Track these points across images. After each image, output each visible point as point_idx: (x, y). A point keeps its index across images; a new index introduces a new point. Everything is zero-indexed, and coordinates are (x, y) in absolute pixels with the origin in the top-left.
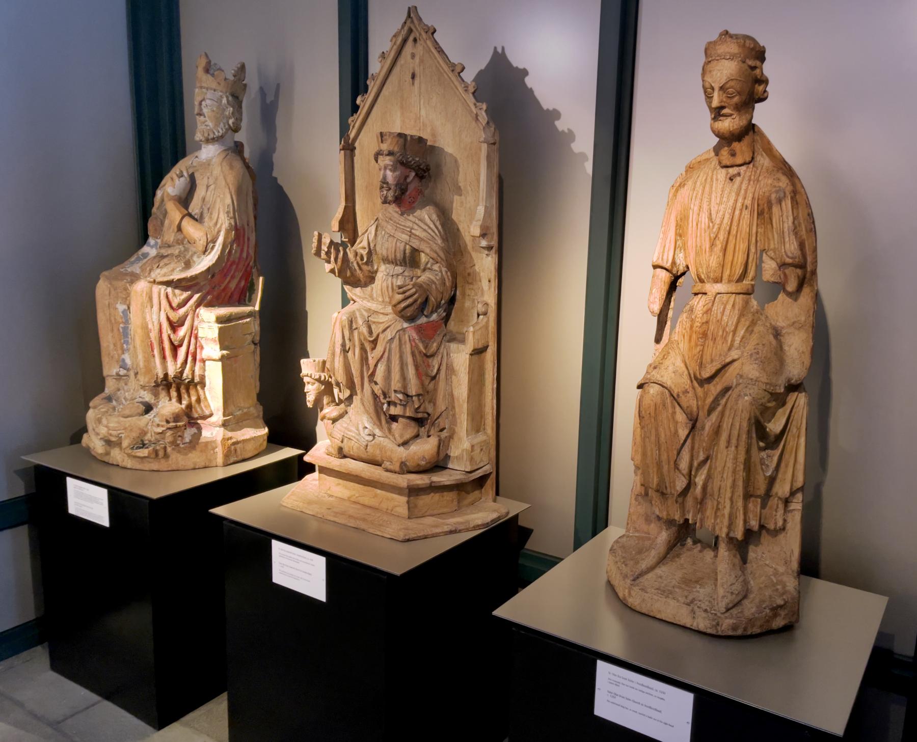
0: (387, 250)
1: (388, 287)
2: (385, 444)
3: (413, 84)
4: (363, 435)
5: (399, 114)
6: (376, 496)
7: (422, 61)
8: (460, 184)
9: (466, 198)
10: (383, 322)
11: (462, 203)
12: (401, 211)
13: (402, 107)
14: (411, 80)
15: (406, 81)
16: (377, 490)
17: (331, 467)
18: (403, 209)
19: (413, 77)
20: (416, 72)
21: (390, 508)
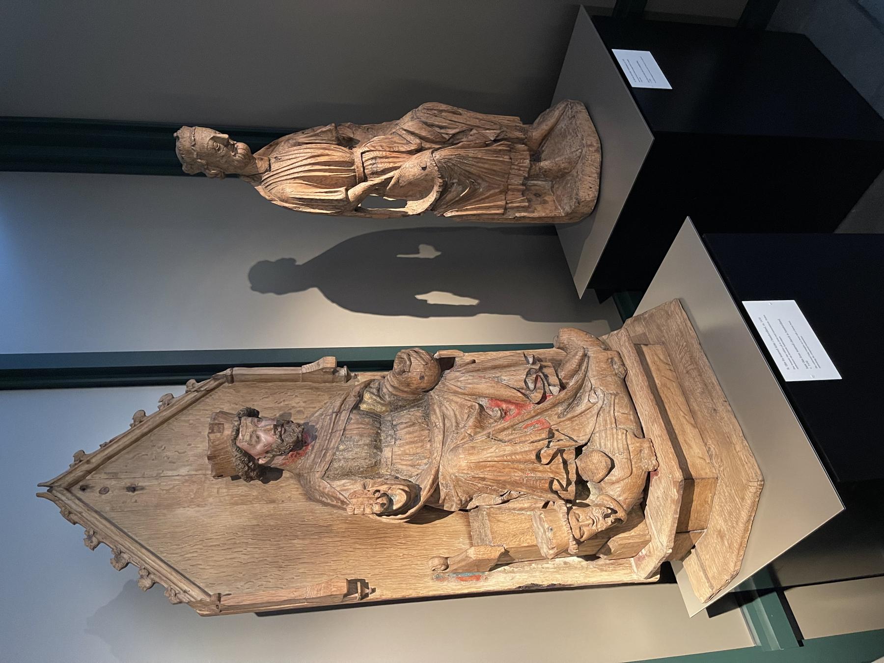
0: (361, 436)
1: (410, 433)
2: (595, 373)
3: (142, 488)
4: (600, 403)
5: (180, 511)
6: (664, 385)
7: (115, 476)
8: (277, 415)
9: (293, 407)
10: (453, 410)
11: (299, 412)
12: (311, 442)
13: (170, 507)
14: (136, 492)
15: (136, 501)
16: (657, 385)
17: (665, 432)
18: (310, 440)
19: (133, 489)
20: (129, 485)
21: (667, 367)
